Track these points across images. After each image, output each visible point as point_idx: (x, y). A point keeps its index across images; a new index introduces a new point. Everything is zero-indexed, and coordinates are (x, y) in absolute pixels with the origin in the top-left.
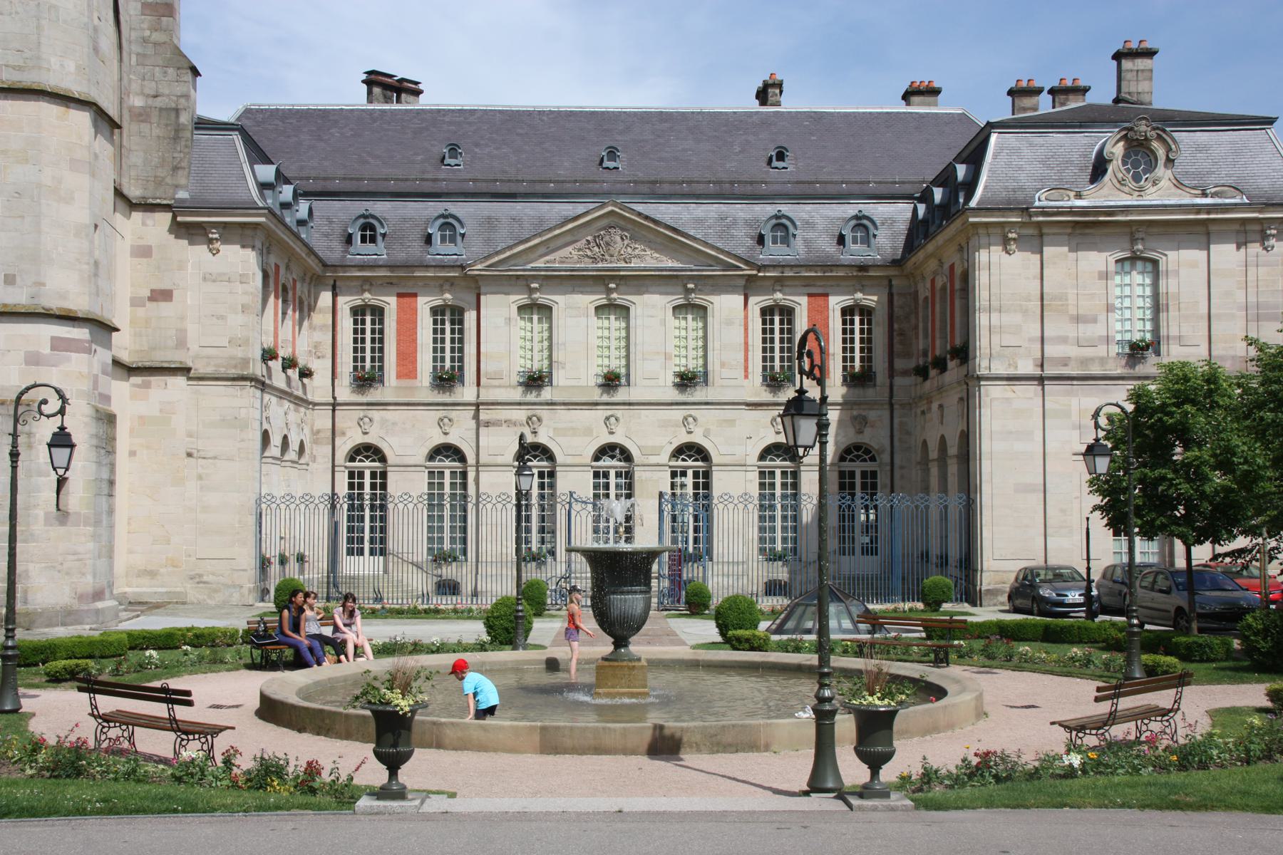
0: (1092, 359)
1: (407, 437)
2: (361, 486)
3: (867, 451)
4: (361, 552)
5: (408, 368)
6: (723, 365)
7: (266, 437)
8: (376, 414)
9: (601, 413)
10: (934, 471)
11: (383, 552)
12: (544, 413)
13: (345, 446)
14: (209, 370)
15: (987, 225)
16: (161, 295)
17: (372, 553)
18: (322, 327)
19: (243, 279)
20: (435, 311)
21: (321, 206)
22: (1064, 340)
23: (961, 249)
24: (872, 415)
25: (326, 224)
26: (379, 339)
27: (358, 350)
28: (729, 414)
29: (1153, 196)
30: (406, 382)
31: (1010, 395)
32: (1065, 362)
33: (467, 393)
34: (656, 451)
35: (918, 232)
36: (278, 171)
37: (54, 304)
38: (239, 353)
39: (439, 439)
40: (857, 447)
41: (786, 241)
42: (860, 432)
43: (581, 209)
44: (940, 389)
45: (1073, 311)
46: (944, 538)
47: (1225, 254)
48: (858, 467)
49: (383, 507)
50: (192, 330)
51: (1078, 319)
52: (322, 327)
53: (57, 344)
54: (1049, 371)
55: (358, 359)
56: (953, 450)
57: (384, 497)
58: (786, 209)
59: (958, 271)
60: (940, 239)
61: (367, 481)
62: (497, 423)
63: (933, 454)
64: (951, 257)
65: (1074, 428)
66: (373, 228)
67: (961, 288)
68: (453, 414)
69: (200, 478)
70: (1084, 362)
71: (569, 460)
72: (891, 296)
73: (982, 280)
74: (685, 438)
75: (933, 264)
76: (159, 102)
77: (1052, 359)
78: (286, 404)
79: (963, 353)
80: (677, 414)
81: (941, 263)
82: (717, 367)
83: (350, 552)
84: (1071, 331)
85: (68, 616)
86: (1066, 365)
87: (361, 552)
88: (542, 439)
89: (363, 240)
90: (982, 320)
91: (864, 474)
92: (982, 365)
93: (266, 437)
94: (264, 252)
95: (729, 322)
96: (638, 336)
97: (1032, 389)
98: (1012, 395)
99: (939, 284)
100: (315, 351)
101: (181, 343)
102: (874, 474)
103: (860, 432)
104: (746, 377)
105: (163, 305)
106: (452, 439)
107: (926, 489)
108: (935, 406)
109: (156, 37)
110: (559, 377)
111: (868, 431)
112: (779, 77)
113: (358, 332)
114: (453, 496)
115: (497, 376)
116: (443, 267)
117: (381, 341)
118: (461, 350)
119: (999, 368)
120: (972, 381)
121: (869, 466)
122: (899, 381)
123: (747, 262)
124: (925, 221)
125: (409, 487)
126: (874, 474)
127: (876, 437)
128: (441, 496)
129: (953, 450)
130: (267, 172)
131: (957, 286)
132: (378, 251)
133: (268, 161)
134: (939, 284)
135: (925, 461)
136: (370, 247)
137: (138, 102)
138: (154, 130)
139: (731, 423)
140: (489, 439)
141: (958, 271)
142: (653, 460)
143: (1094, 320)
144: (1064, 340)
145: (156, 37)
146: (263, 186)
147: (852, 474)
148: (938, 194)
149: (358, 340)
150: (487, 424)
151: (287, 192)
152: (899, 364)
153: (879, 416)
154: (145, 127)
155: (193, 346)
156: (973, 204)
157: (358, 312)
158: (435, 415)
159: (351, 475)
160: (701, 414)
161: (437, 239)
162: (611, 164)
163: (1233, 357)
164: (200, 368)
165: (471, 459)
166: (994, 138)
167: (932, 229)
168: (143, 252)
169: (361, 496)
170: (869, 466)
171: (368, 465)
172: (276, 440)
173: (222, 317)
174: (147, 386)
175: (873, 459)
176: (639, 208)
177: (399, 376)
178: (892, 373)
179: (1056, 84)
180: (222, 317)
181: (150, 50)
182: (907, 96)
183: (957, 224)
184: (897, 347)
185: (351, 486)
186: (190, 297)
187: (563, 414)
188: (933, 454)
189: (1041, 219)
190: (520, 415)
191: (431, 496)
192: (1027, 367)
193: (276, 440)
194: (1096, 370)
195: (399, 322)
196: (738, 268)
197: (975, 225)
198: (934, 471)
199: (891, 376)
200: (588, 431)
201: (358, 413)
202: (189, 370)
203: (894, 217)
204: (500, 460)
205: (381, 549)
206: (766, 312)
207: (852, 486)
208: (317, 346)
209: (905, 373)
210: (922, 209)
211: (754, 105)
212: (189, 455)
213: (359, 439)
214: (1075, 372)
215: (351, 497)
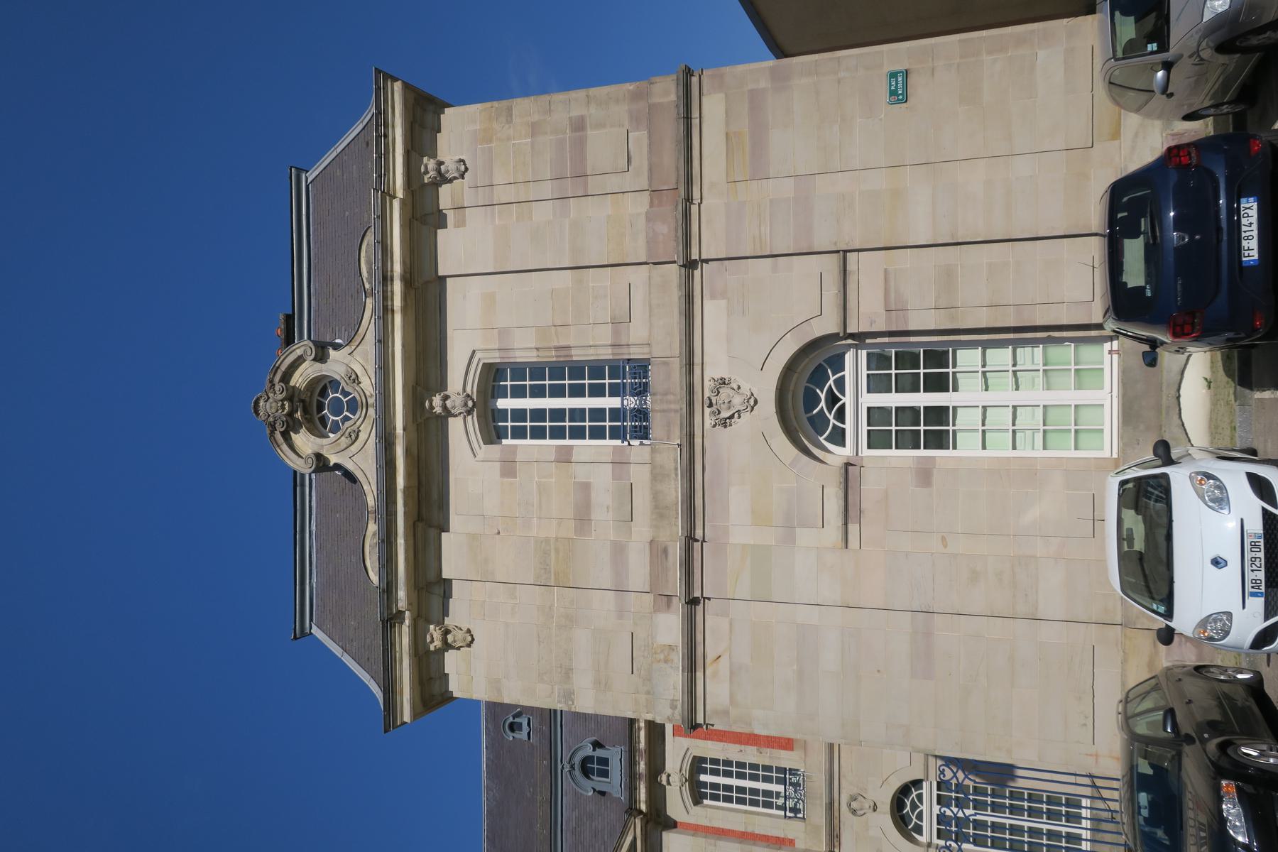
0: (656, 496)
31: (724, 664)
32: (658, 552)
47: (455, 249)
51: (583, 518)
65: (789, 539)
70: (659, 511)
86: (665, 551)
98: (724, 662)
104: (792, 842)
123: (623, 834)
143: (586, 487)
163: (649, 218)
194: (674, 491)
196: (635, 838)
214: (679, 529)
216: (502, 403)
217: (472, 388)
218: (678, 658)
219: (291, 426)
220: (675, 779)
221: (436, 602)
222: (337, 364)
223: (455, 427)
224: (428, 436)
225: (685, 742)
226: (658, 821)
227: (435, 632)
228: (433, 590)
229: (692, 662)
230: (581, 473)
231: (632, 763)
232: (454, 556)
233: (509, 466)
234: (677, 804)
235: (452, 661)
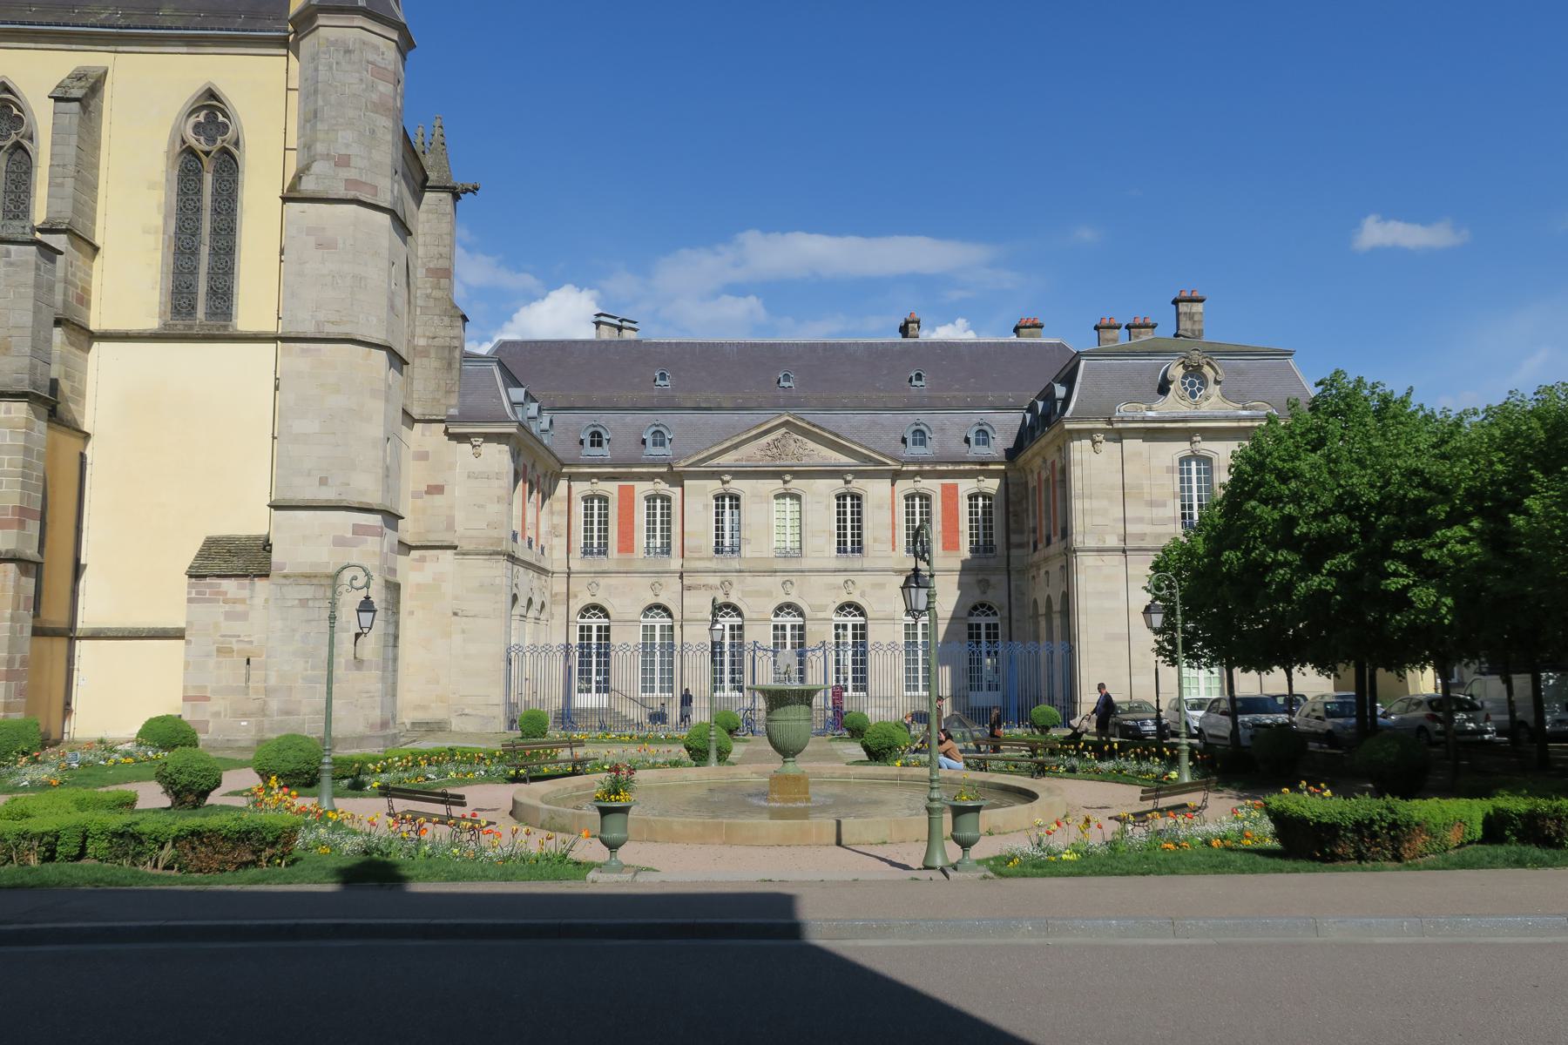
1: (626, 601)
2: (590, 637)
3: (990, 608)
4: (589, 691)
5: (627, 544)
6: (875, 540)
7: (515, 598)
8: (603, 581)
9: (779, 579)
10: (1043, 623)
11: (607, 690)
12: (733, 577)
13: (577, 605)
14: (471, 547)
15: (1079, 431)
16: (435, 490)
17: (598, 690)
18: (559, 513)
19: (498, 476)
20: (648, 499)
21: (560, 417)
22: (1140, 520)
23: (1060, 449)
24: (993, 579)
25: (560, 431)
26: (604, 523)
27: (588, 530)
28: (879, 578)
29: (1206, 408)
30: (626, 556)
32: (1142, 537)
33: (675, 563)
34: (823, 608)
35: (1025, 437)
36: (527, 394)
37: (354, 500)
38: (495, 534)
39: (652, 600)
40: (983, 605)
41: (923, 443)
42: (984, 592)
43: (763, 418)
44: (1046, 559)
45: (1147, 497)
46: (1051, 677)
48: (983, 621)
49: (607, 655)
50: (459, 517)
51: (1152, 504)
52: (559, 513)
53: (358, 530)
54: (1130, 544)
55: (588, 536)
56: (1057, 607)
57: (607, 646)
58: (923, 417)
59: (1058, 466)
60: (1043, 442)
61: (594, 633)
62: (697, 587)
63: (1042, 610)
64: (1052, 455)
66: (600, 435)
67: (1060, 478)
68: (662, 580)
69: (463, 632)
71: (755, 616)
72: (1007, 485)
73: (1076, 473)
74: (846, 598)
75: (1038, 461)
76: (437, 342)
77: (1132, 535)
78: (531, 573)
79: (1066, 533)
80: (840, 579)
81: (1045, 461)
82: (871, 542)
83: (580, 691)
84: (1146, 512)
85: (360, 740)
87: (589, 691)
88: (733, 599)
89: (592, 444)
90: (1077, 505)
91: (988, 626)
92: (1078, 540)
93: (515, 598)
94: (515, 456)
95: (880, 507)
96: (809, 518)
97: (1118, 559)
99: (1044, 475)
100: (553, 532)
101: (450, 527)
102: (996, 626)
103: (984, 592)
105: (437, 497)
106: (661, 600)
107: (1037, 638)
108: (1042, 572)
109: (437, 294)
110: (746, 551)
111: (990, 593)
112: (916, 317)
113: (588, 515)
114: (662, 645)
115: (698, 549)
116: (655, 465)
117: (606, 523)
118: (669, 530)
119: (1091, 543)
120: (1069, 552)
121: (992, 620)
122: (1014, 552)
123: (892, 459)
124: (1032, 427)
125: (627, 638)
126: (996, 626)
127: (996, 597)
128: (653, 645)
129: (1057, 607)
130: (518, 394)
131: (1058, 477)
132: (605, 451)
133: (518, 385)
134: (1044, 475)
135: (1036, 615)
136: (596, 451)
137: (421, 342)
138: (432, 363)
139: (881, 586)
140: (689, 599)
141: (1058, 466)
142: (821, 615)
143: (1164, 505)
144: (1140, 520)
145: (437, 294)
146: (513, 404)
147: (978, 626)
148: (1040, 404)
149: (588, 523)
150: (689, 588)
151: (533, 409)
152: (1015, 539)
153: (998, 579)
154: (425, 361)
155: (460, 529)
156: (1068, 414)
157: (588, 499)
158: (648, 581)
159: (582, 629)
160: (861, 579)
161: (649, 442)
162: (786, 384)
164: (464, 545)
165: (677, 615)
166: (1082, 363)
167: (1038, 433)
168: (423, 456)
169: (589, 645)
170: (992, 620)
171: (595, 622)
172: (523, 601)
173: (482, 506)
174: (423, 559)
175: (995, 614)
176: (809, 418)
177: (620, 551)
178: (1008, 546)
179: (1131, 322)
180: (482, 506)
181: (431, 303)
182: (1016, 330)
183: (1056, 430)
184: (1012, 525)
185: (582, 637)
186: (458, 490)
187: (749, 579)
188: (1042, 610)
189: (1120, 425)
190: (715, 580)
191: (644, 645)
192: (1113, 541)
193: (523, 601)
195: (620, 508)
197: (1070, 431)
198: (1043, 623)
199: (1008, 548)
200: (769, 594)
201: (587, 579)
202: (455, 548)
203: (1006, 425)
204: (699, 616)
205: (604, 687)
206: (909, 498)
207: (979, 636)
208: (554, 527)
209: (1020, 546)
210: (1028, 416)
211: (899, 338)
212: (455, 614)
213: (589, 600)
214: (1149, 546)
215: (581, 646)
216: (1194, 464)
217: (1203, 453)
218: (1100, 545)
219: (1185, 367)
220: (919, 485)
221: (1112, 436)
222: (1214, 390)
223: (1186, 445)
224: (1187, 435)
225: (939, 490)
226: (895, 476)
227: (1100, 437)
228: (1118, 436)
229: (1099, 550)
230: (1170, 503)
231: (929, 463)
232: (1131, 445)
233: (1170, 470)
234: (905, 486)
235: (1087, 443)
